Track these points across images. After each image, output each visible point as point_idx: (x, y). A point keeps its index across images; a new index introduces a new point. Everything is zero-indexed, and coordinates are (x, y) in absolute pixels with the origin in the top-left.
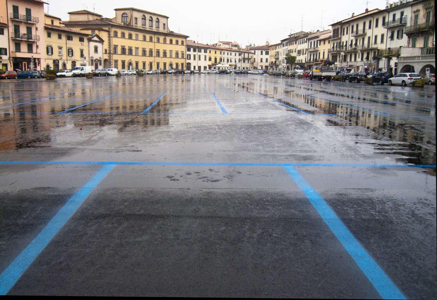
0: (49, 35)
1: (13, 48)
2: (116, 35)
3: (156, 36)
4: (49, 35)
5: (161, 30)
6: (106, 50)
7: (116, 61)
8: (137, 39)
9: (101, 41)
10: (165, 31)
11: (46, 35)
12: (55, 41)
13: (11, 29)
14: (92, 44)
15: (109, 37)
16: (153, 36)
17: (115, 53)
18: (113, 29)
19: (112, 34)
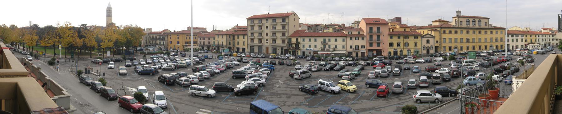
0: (391, 38)
1: (368, 45)
2: (444, 32)
3: (478, 31)
4: (391, 38)
5: (483, 26)
6: (437, 42)
7: (445, 47)
8: (462, 33)
9: (434, 37)
10: (487, 27)
11: (389, 37)
12: (395, 40)
13: (368, 37)
14: (425, 40)
15: (440, 34)
16: (476, 31)
17: (445, 42)
18: (442, 30)
19: (442, 32)
